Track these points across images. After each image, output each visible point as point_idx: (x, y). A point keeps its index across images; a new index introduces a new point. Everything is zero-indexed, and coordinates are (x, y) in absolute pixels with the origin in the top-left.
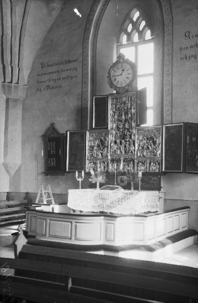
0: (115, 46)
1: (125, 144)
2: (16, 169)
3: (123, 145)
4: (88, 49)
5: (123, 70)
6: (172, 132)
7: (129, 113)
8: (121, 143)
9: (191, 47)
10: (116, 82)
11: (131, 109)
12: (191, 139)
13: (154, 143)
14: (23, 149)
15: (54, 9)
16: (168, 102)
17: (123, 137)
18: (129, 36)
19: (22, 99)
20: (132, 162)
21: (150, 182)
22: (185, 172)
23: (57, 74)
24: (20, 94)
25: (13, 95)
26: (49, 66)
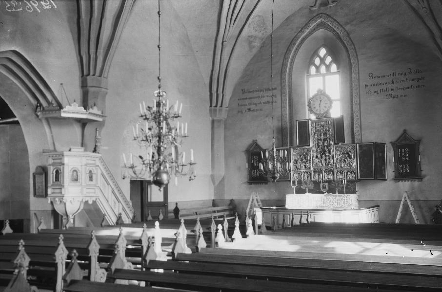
0: (306, 76)
2: (220, 180)
3: (324, 159)
4: (286, 80)
5: (321, 101)
6: (364, 148)
8: (322, 157)
9: (374, 85)
10: (316, 109)
11: (329, 131)
12: (379, 154)
13: (350, 157)
14: (226, 164)
15: (254, 47)
18: (318, 68)
19: (223, 119)
21: (350, 189)
22: (376, 179)
23: (257, 99)
24: (223, 115)
25: (217, 117)
26: (249, 92)
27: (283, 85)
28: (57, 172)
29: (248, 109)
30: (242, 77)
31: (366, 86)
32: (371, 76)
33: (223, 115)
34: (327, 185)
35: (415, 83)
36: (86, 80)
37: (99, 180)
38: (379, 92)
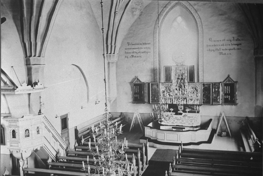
6: (206, 86)
7: (184, 75)
9: (212, 46)
11: (184, 74)
17: (180, 87)
23: (138, 49)
25: (112, 60)
26: (132, 45)
27: (155, 41)
28: (14, 132)
29: (132, 56)
30: (128, 34)
31: (207, 46)
32: (210, 39)
33: (114, 58)
34: (182, 107)
35: (236, 47)
36: (29, 60)
37: (44, 132)
38: (215, 50)
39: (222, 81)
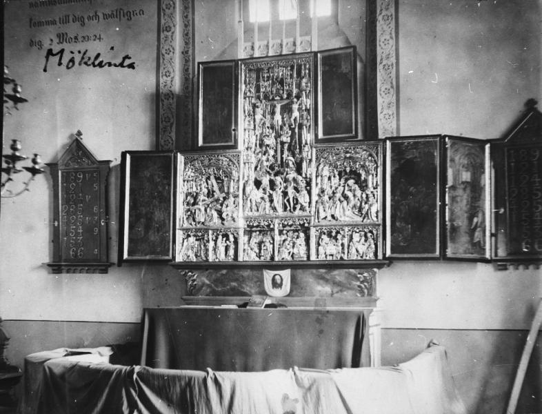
1: (286, 188)
7: (295, 107)
8: (272, 184)
13: (363, 185)
16: (389, 87)
20: (302, 235)
39: (495, 132)
